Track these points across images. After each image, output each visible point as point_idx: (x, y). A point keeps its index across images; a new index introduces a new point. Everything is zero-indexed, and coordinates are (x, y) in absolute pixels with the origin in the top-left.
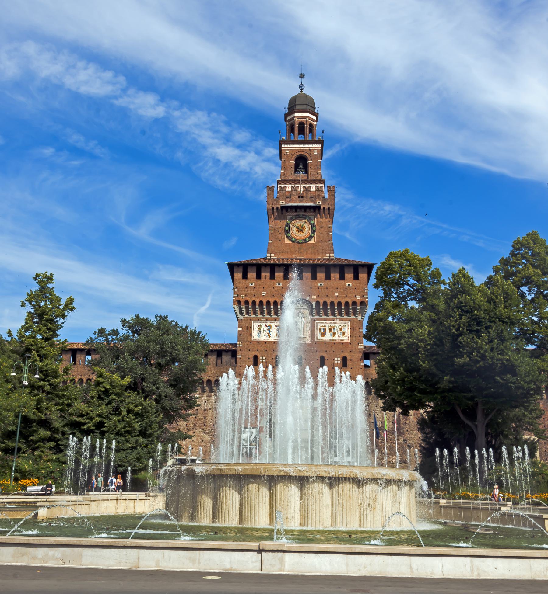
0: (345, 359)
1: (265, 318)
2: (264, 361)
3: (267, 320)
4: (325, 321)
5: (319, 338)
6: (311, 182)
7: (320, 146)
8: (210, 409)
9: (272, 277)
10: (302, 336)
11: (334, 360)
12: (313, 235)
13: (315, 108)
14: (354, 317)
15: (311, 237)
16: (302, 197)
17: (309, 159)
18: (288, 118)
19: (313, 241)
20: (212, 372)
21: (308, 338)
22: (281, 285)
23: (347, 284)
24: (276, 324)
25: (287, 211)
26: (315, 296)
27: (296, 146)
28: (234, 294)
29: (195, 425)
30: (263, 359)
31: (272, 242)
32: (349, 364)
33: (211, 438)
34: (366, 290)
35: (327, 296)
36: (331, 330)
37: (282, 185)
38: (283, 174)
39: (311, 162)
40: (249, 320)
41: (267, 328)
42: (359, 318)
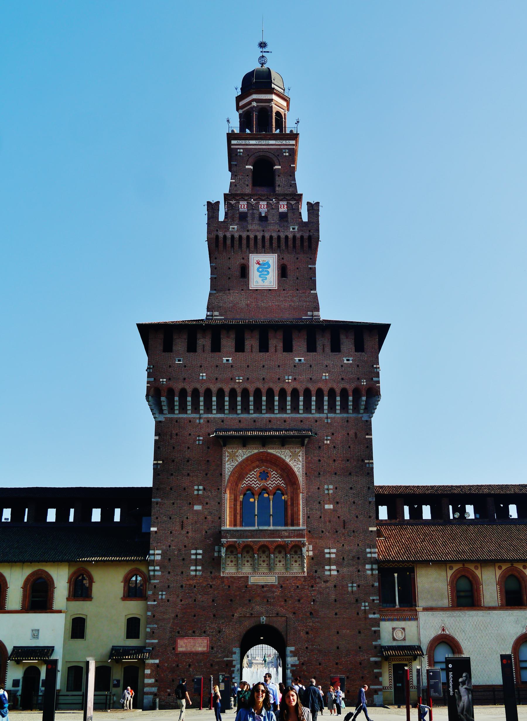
7: (293, 142)
9: (216, 348)
17: (276, 162)
18: (241, 104)
22: (230, 362)
31: (215, 292)
34: (376, 368)
39: (280, 167)
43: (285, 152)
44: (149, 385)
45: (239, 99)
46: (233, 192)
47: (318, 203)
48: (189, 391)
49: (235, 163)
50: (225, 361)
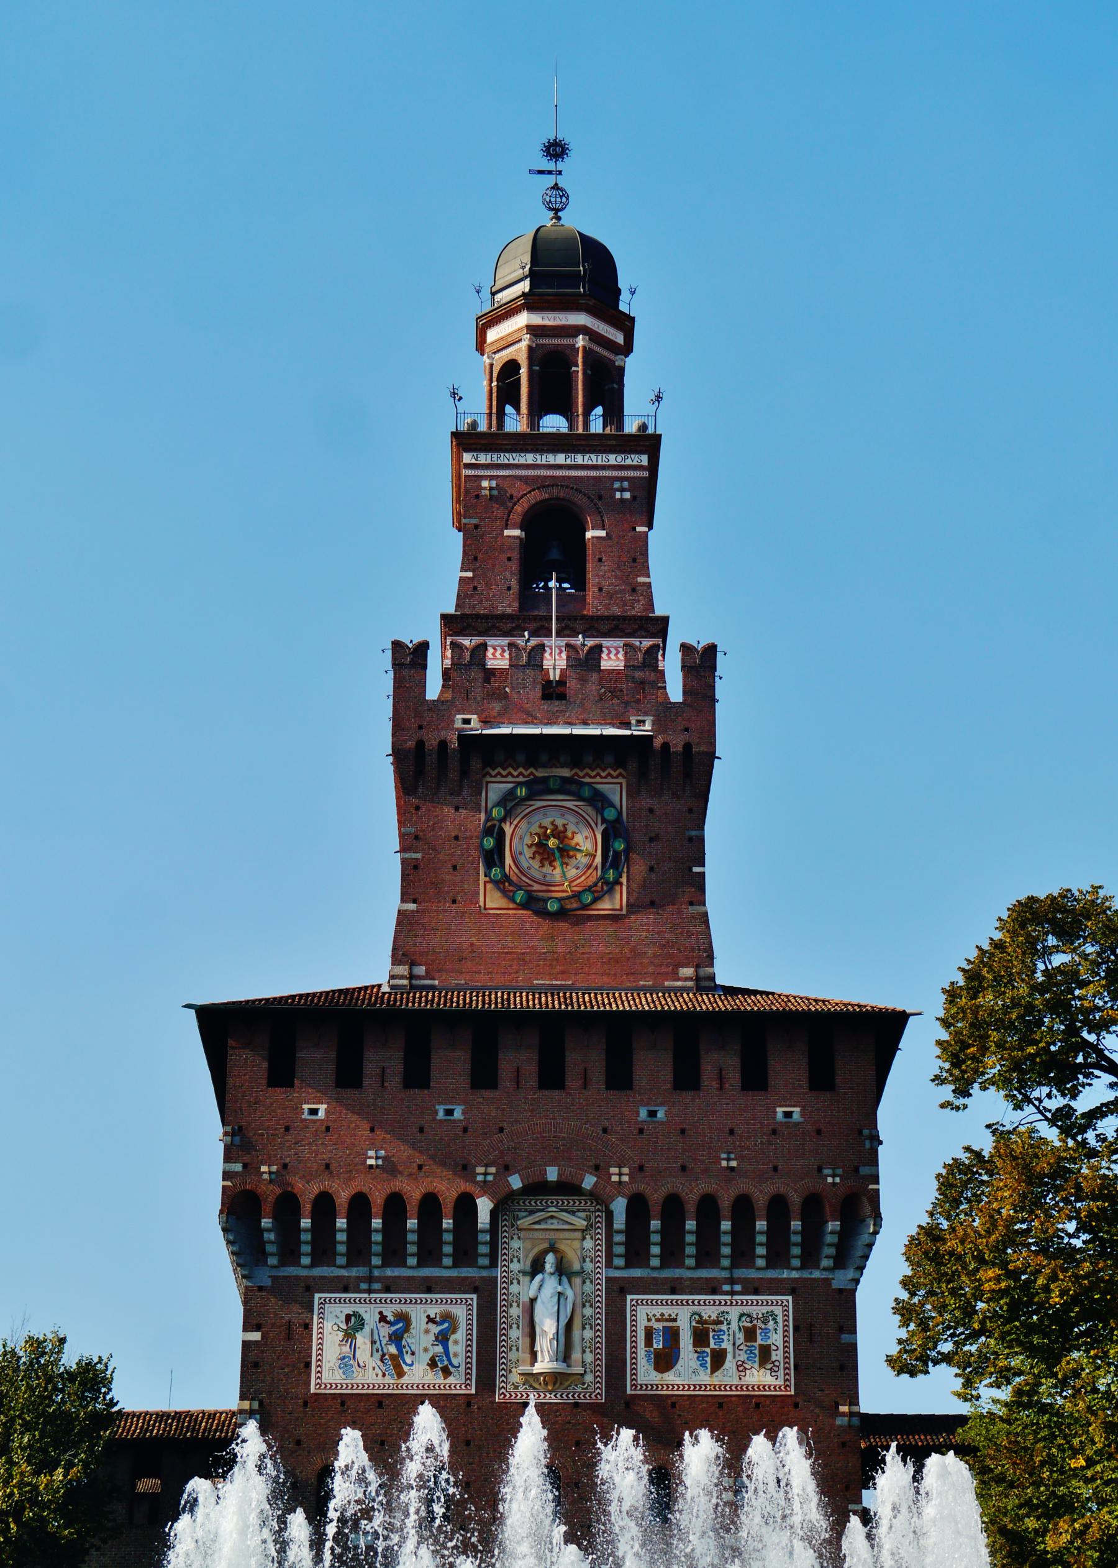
3: (387, 1290)
4: (673, 1291)
6: (604, 628)
7: (644, 460)
12: (611, 875)
13: (619, 292)
14: (817, 1274)
16: (562, 697)
18: (492, 335)
21: (589, 1378)
22: (458, 1114)
24: (434, 1311)
25: (490, 762)
26: (626, 1170)
27: (529, 458)
28: (228, 1158)
31: (412, 906)
35: (683, 1168)
36: (700, 1337)
37: (466, 642)
38: (466, 590)
39: (603, 533)
41: (385, 1331)
42: (840, 1279)
43: (622, 490)
44: (229, 1183)
46: (467, 611)
47: (711, 649)
49: (475, 521)
50: (441, 1115)
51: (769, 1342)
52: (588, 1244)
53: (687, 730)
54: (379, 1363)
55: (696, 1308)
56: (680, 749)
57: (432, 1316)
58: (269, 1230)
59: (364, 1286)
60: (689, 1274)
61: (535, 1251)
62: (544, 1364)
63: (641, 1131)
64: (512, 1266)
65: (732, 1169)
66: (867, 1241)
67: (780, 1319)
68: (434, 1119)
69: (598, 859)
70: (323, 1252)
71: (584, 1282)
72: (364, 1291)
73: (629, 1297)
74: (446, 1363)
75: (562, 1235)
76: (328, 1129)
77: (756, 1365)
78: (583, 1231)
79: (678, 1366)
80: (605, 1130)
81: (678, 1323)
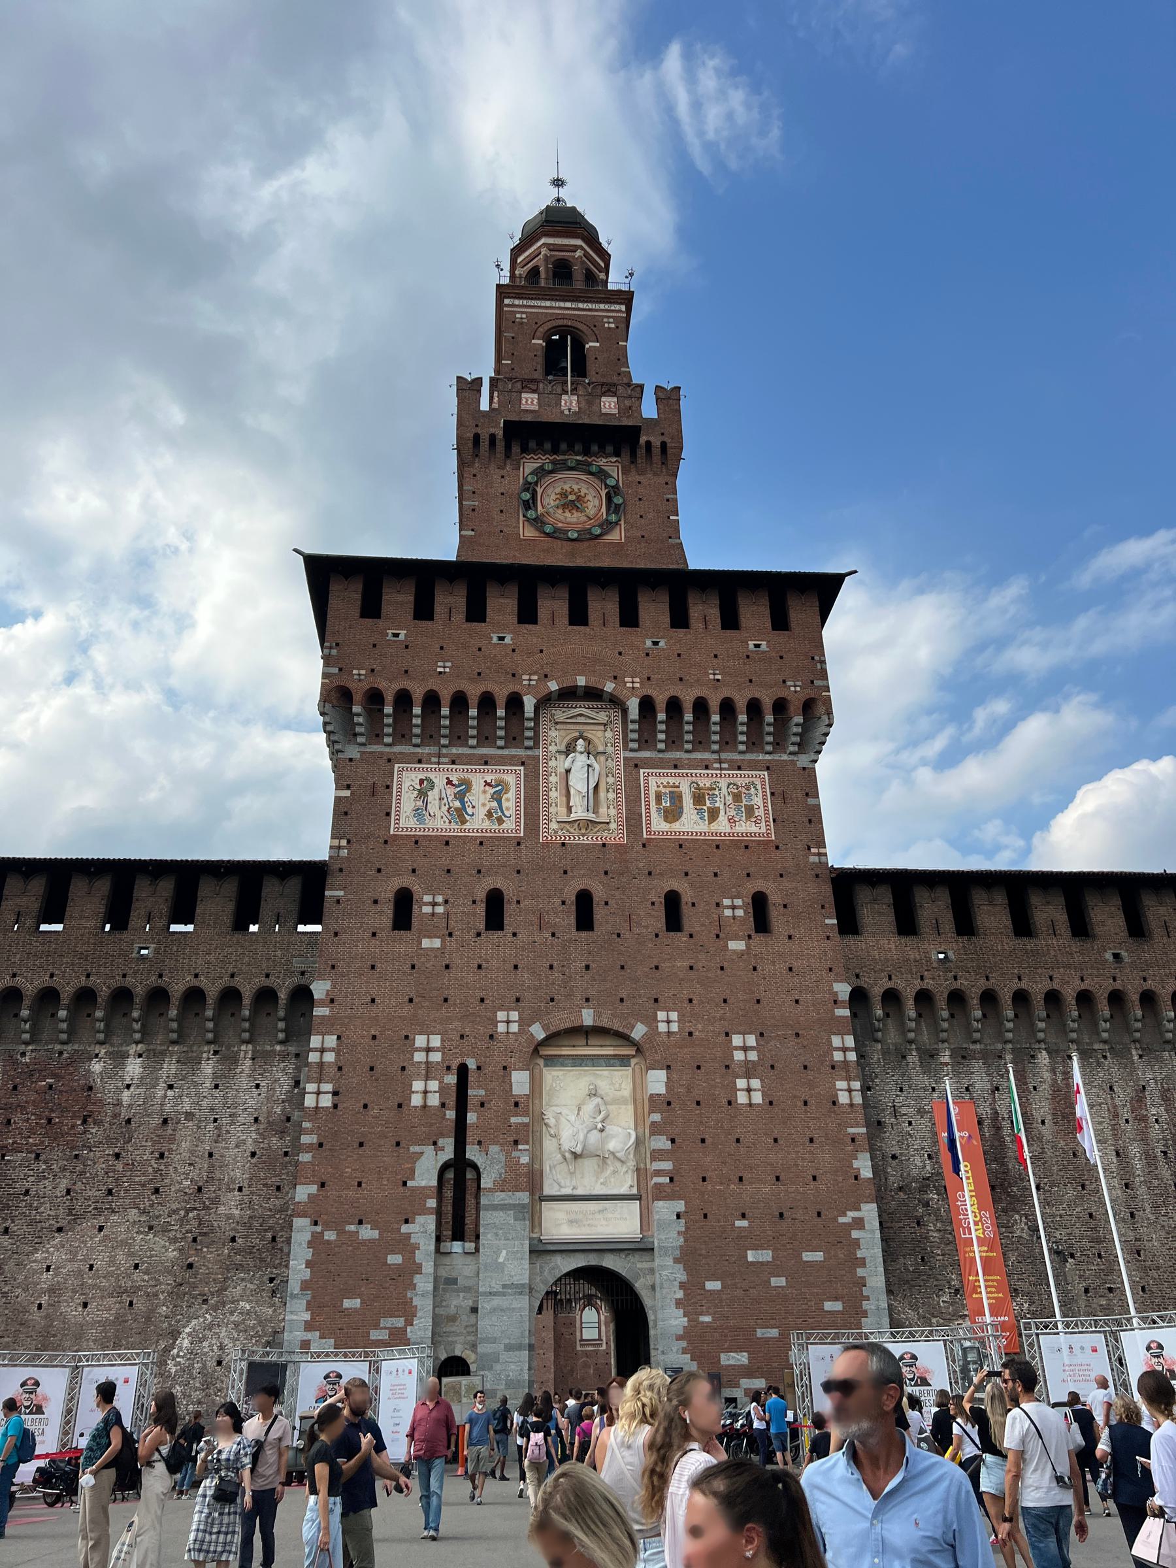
0: (759, 903)
1: (445, 756)
2: (440, 910)
3: (453, 762)
4: (676, 767)
5: (658, 825)
8: (189, 1116)
9: (476, 612)
10: (592, 817)
11: (718, 905)
12: (613, 518)
14: (785, 757)
15: (608, 526)
19: (615, 536)
20: (211, 958)
21: (613, 826)
22: (508, 640)
23: (751, 643)
25: (525, 450)
28: (326, 665)
29: (110, 1192)
30: (434, 904)
31: (473, 533)
32: (777, 918)
33: (181, 1250)
35: (681, 679)
36: (698, 799)
40: (383, 762)
41: (451, 791)
44: (327, 681)
45: (516, 251)
48: (418, 695)
51: (752, 803)
52: (609, 734)
53: (663, 434)
54: (446, 813)
55: (694, 779)
56: (658, 444)
57: (489, 781)
58: (358, 715)
59: (434, 760)
60: (687, 756)
61: (568, 738)
62: (579, 813)
63: (647, 654)
64: (550, 748)
65: (718, 680)
66: (824, 731)
67: (759, 787)
68: (490, 643)
69: (604, 509)
70: (402, 736)
71: (607, 760)
72: (435, 763)
73: (642, 771)
74: (500, 814)
75: (588, 727)
76: (407, 647)
77: (744, 818)
78: (605, 725)
79: (682, 819)
80: (620, 654)
81: (681, 789)
